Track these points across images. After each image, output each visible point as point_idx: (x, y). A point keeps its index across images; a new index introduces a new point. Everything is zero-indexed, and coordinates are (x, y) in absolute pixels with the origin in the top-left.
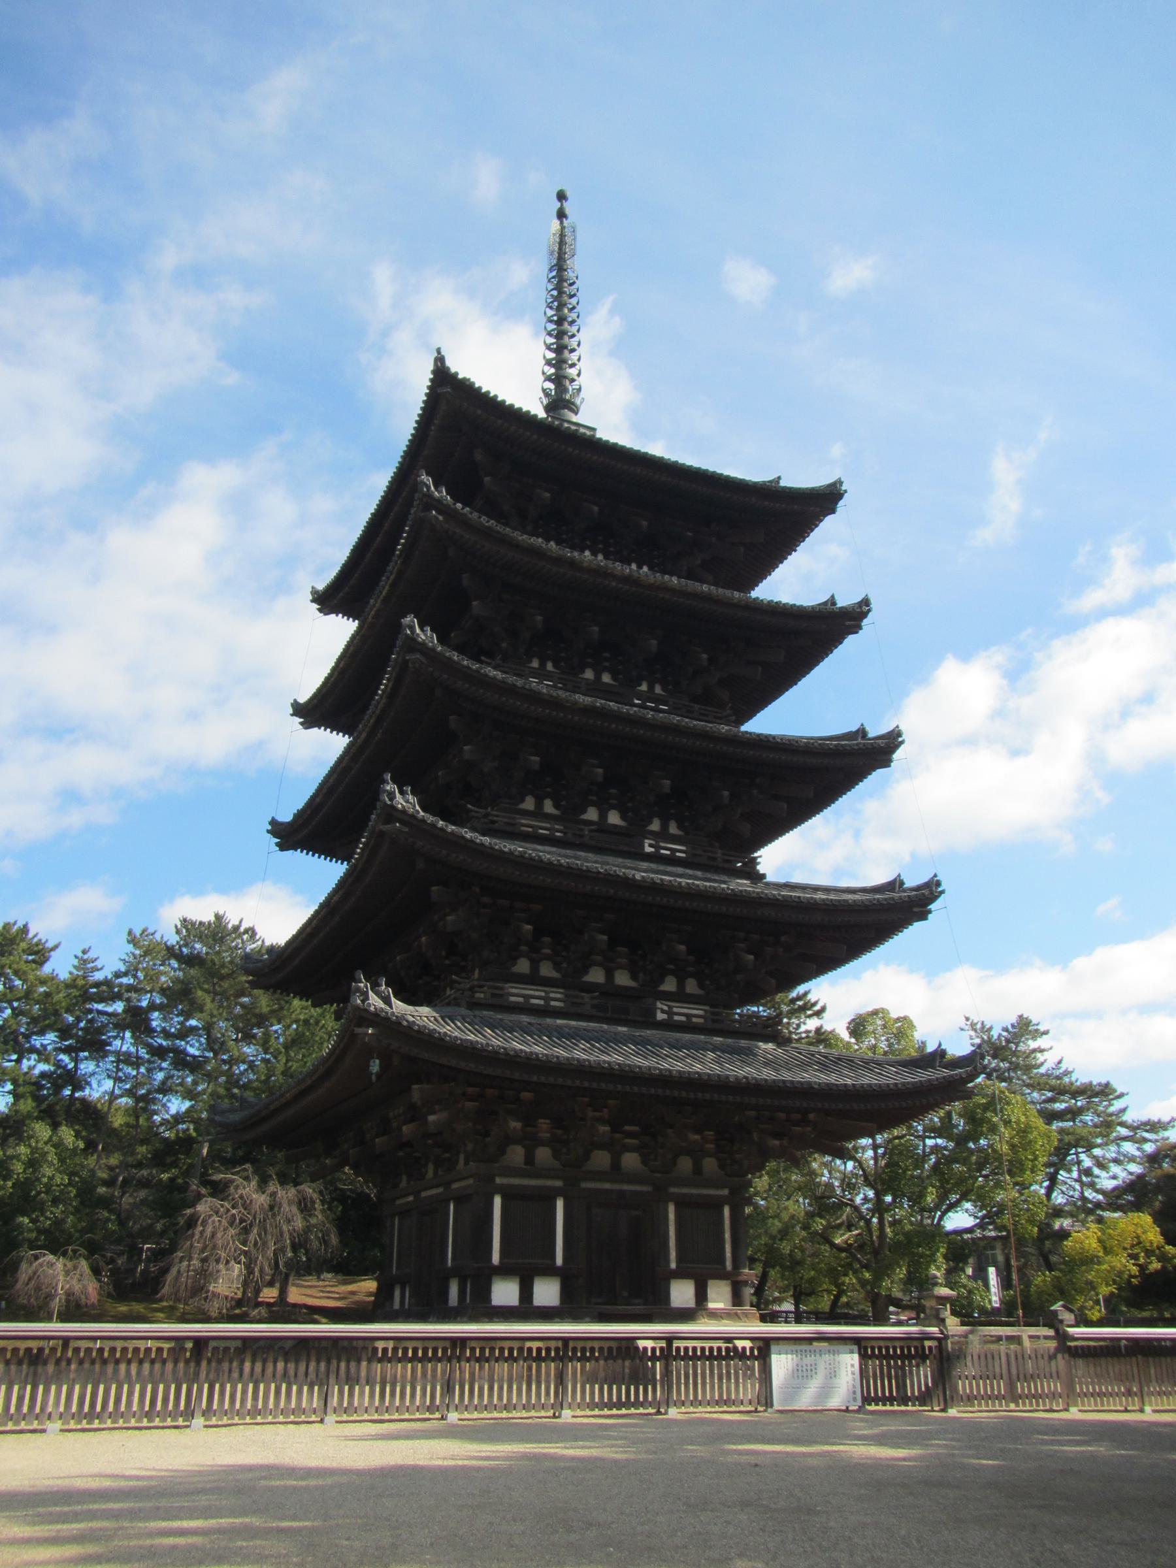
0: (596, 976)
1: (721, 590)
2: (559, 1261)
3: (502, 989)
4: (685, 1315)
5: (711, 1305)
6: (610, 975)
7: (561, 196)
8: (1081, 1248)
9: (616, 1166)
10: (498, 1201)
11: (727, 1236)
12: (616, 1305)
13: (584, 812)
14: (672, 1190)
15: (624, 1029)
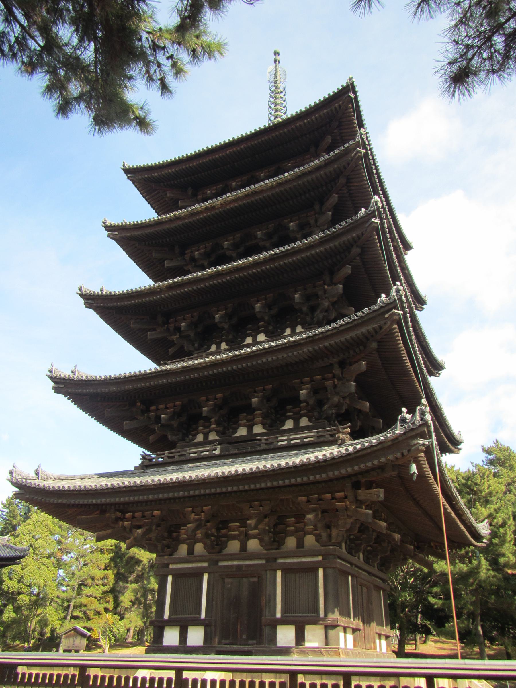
0: (242, 432)
1: (257, 185)
2: (203, 616)
3: (164, 454)
4: (285, 651)
5: (307, 644)
6: (250, 428)
7: (276, 53)
8: (459, 576)
9: (243, 548)
10: (170, 579)
11: (321, 591)
12: (236, 644)
13: (244, 341)
14: (280, 561)
15: (230, 460)
